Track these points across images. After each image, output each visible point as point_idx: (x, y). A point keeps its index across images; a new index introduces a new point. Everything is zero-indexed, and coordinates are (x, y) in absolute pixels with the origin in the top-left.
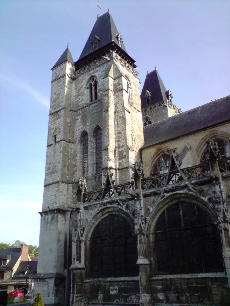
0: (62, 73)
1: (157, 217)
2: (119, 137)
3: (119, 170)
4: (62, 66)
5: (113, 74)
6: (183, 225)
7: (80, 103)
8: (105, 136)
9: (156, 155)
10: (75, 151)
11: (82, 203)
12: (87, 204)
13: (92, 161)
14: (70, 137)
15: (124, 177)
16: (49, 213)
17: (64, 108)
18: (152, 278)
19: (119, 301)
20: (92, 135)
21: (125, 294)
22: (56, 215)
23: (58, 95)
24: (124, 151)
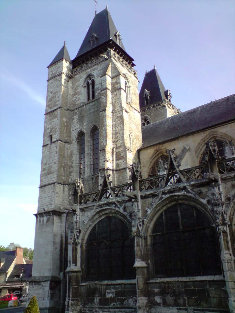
0: (59, 71)
1: (155, 219)
2: (116, 138)
3: (116, 171)
4: (59, 64)
5: (110, 73)
6: (181, 227)
7: (77, 103)
8: (102, 136)
9: (155, 156)
10: (72, 152)
11: (79, 204)
12: (83, 206)
13: (89, 161)
14: (66, 137)
15: (121, 178)
16: (44, 215)
17: (60, 108)
18: (149, 281)
19: (115, 304)
20: (89, 135)
21: (122, 298)
22: (51, 217)
23: (55, 93)
24: (122, 151)
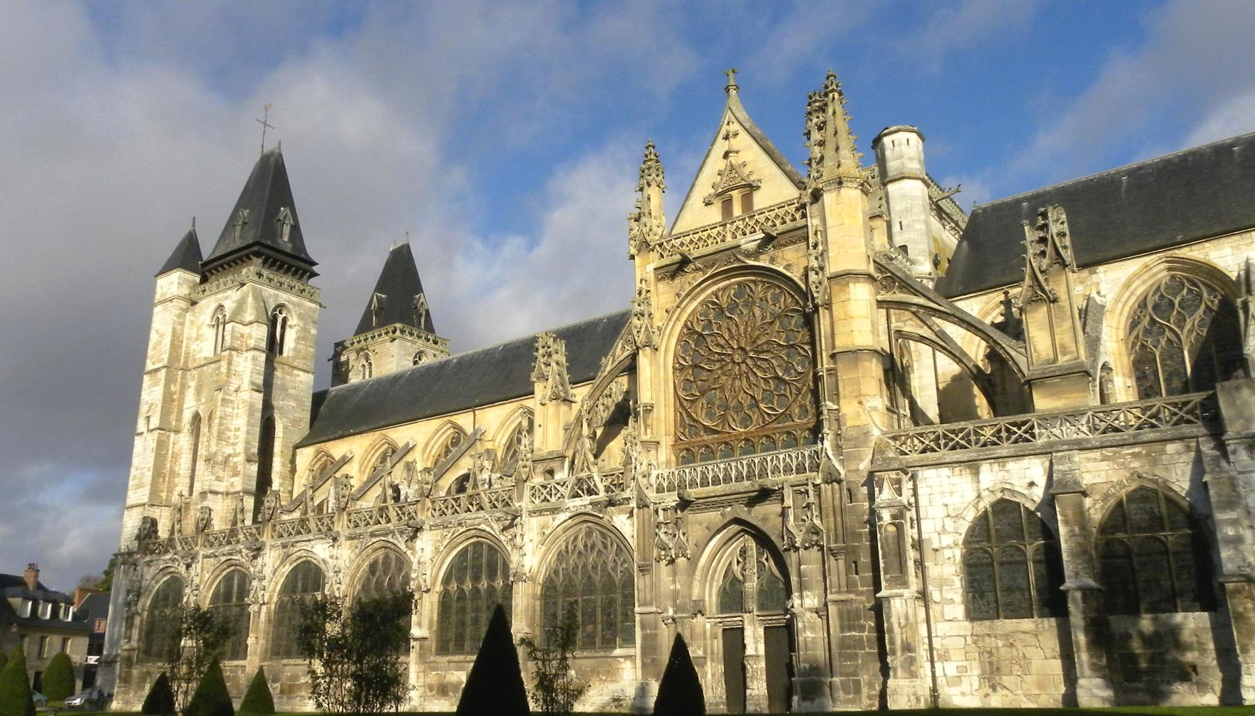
7: (197, 356)
